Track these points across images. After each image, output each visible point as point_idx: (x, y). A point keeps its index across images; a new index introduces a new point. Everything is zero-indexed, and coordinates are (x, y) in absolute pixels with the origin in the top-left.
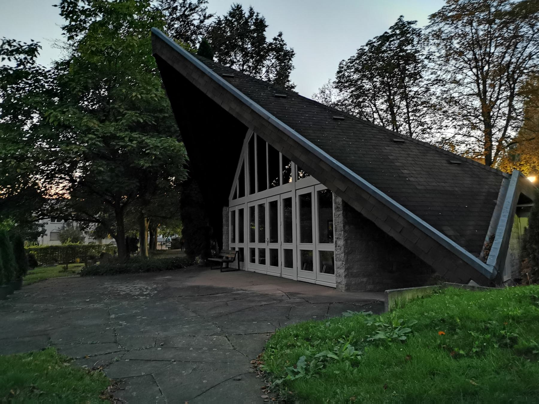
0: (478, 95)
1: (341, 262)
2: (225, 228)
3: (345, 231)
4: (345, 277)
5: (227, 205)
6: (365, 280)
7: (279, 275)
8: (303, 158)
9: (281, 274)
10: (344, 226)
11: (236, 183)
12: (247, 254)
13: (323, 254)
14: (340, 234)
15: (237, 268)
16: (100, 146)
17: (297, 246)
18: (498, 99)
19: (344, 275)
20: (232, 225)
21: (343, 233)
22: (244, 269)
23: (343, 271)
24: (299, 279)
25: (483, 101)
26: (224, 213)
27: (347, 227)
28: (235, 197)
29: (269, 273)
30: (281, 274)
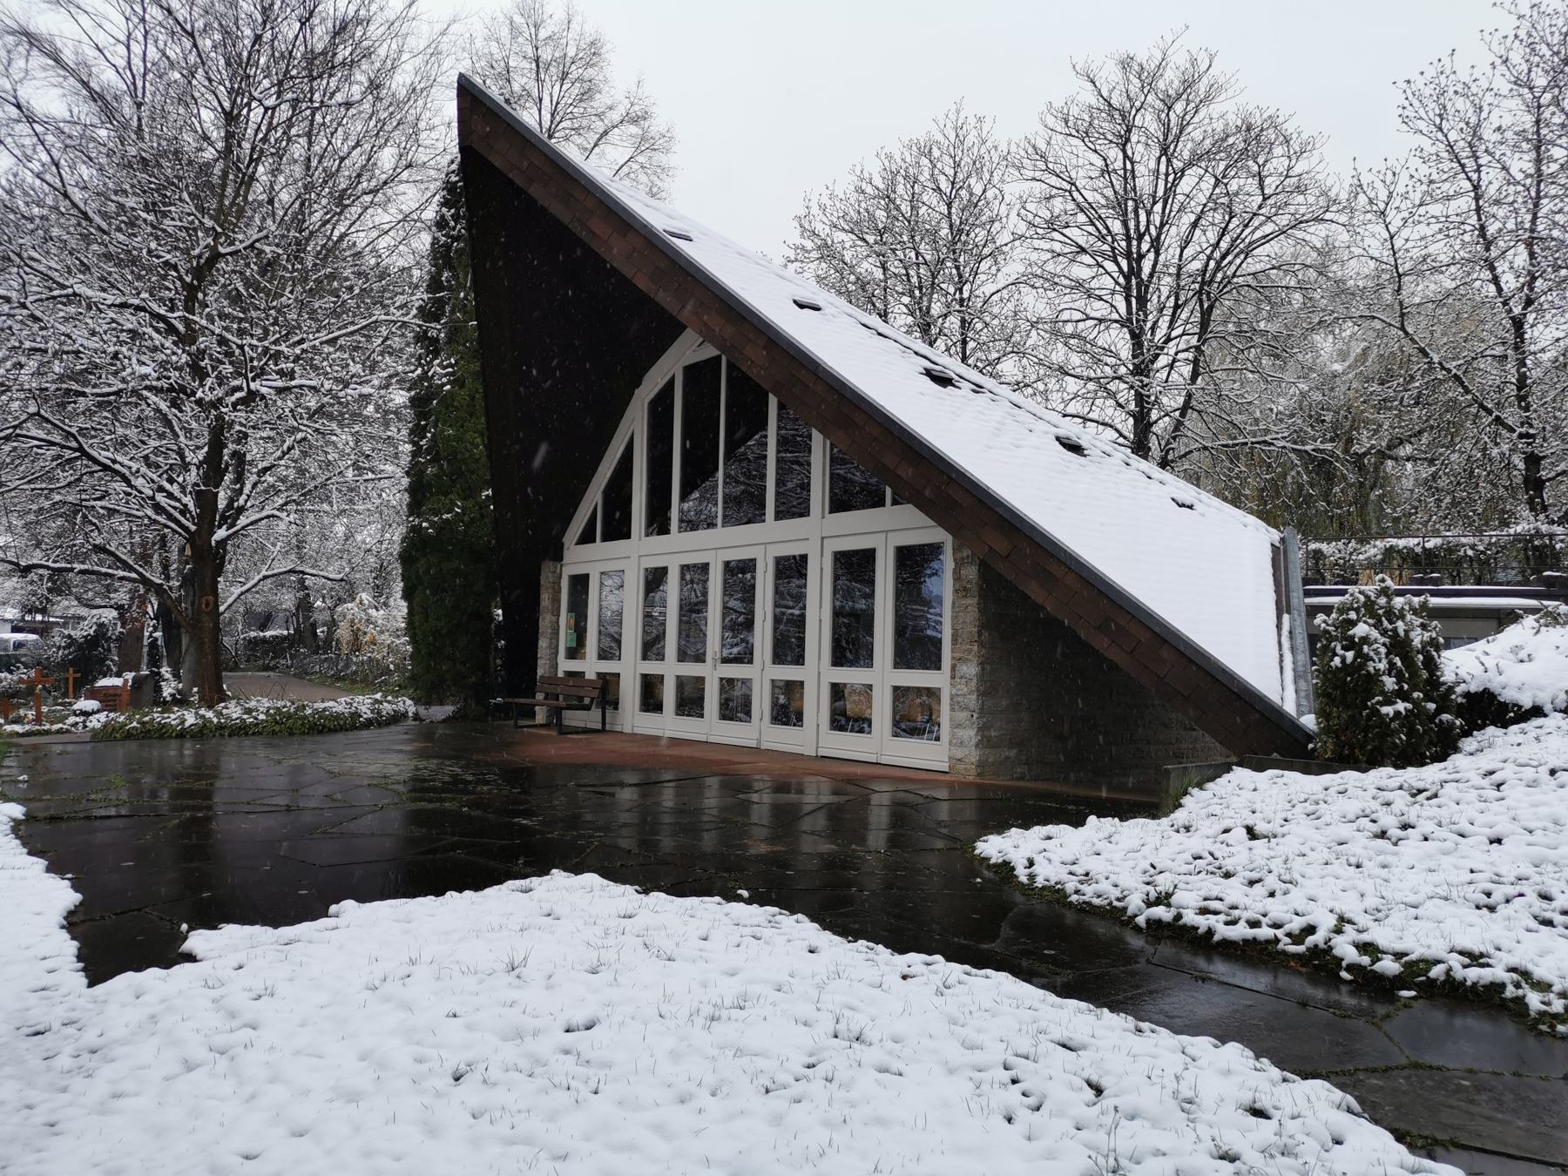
0: (1124, 323)
1: (966, 714)
2: (545, 623)
3: (982, 645)
4: (977, 746)
5: (558, 556)
6: (1013, 753)
7: (753, 744)
8: (907, 472)
9: (759, 741)
10: (980, 634)
11: (594, 497)
12: (630, 692)
13: (727, 684)
14: (970, 651)
15: (599, 726)
16: (894, 493)
17: (762, 674)
18: (1168, 339)
19: (974, 741)
20: (570, 610)
21: (975, 648)
22: (619, 729)
23: (972, 732)
24: (822, 752)
25: (1136, 337)
26: (546, 578)
27: (986, 634)
28: (587, 537)
29: (712, 739)
30: (759, 741)
